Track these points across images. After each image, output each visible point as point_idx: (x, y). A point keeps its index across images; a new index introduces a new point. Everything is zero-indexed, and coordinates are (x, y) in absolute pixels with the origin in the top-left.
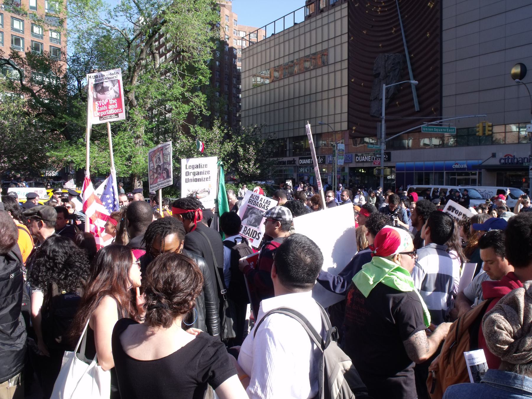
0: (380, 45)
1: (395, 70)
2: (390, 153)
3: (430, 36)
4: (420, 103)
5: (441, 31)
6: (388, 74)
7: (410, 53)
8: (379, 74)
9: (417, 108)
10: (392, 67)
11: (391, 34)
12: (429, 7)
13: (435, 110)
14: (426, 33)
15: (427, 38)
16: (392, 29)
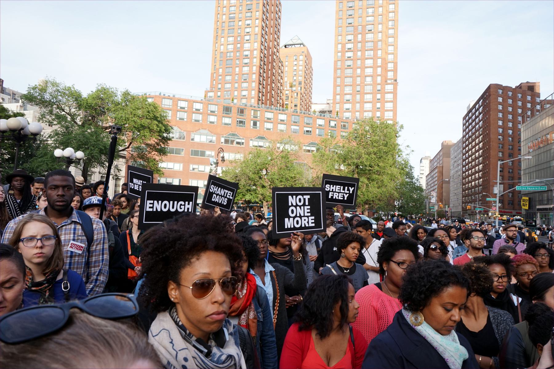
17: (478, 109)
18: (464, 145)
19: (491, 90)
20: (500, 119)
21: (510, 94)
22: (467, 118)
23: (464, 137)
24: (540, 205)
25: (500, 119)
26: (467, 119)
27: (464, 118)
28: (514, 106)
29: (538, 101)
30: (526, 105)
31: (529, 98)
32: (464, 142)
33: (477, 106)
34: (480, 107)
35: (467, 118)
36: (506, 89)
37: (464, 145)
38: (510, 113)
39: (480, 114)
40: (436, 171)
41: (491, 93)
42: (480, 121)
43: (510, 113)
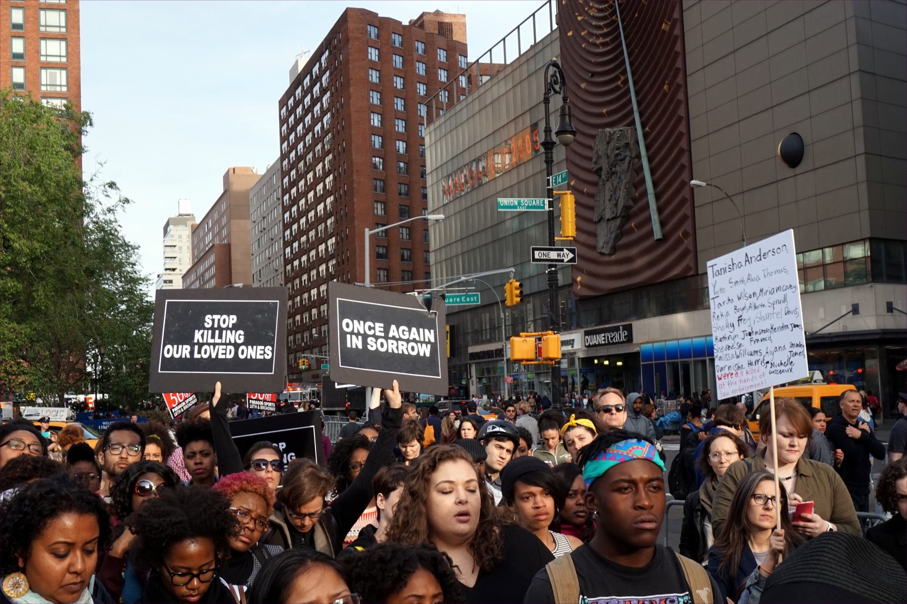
0: (604, 111)
1: (623, 160)
2: (631, 325)
3: (669, 88)
4: (663, 224)
5: (685, 76)
6: (614, 169)
7: (643, 126)
8: (601, 169)
9: (658, 234)
10: (617, 155)
11: (618, 88)
12: (664, 31)
13: (686, 234)
14: (663, 84)
15: (665, 94)
16: (617, 78)
17: (319, 78)
18: (286, 180)
19: (351, 25)
20: (373, 109)
21: (397, 39)
22: (291, 101)
23: (284, 156)
24: (477, 343)
25: (373, 109)
26: (291, 105)
27: (283, 103)
28: (407, 73)
29: (464, 66)
30: (436, 74)
31: (442, 55)
32: (285, 173)
33: (316, 69)
34: (322, 72)
35: (291, 101)
36: (386, 25)
37: (286, 180)
38: (398, 94)
39: (323, 91)
40: (212, 258)
41: (350, 35)
42: (323, 113)
43: (398, 94)
